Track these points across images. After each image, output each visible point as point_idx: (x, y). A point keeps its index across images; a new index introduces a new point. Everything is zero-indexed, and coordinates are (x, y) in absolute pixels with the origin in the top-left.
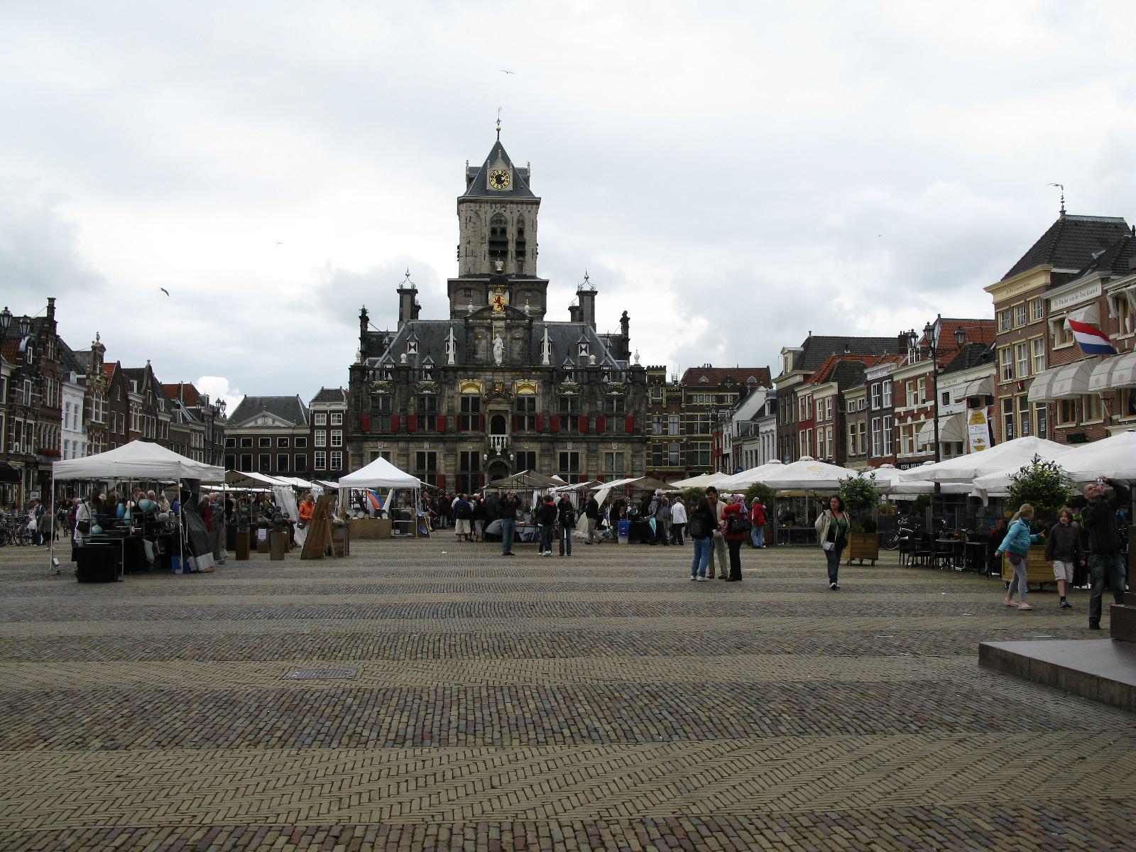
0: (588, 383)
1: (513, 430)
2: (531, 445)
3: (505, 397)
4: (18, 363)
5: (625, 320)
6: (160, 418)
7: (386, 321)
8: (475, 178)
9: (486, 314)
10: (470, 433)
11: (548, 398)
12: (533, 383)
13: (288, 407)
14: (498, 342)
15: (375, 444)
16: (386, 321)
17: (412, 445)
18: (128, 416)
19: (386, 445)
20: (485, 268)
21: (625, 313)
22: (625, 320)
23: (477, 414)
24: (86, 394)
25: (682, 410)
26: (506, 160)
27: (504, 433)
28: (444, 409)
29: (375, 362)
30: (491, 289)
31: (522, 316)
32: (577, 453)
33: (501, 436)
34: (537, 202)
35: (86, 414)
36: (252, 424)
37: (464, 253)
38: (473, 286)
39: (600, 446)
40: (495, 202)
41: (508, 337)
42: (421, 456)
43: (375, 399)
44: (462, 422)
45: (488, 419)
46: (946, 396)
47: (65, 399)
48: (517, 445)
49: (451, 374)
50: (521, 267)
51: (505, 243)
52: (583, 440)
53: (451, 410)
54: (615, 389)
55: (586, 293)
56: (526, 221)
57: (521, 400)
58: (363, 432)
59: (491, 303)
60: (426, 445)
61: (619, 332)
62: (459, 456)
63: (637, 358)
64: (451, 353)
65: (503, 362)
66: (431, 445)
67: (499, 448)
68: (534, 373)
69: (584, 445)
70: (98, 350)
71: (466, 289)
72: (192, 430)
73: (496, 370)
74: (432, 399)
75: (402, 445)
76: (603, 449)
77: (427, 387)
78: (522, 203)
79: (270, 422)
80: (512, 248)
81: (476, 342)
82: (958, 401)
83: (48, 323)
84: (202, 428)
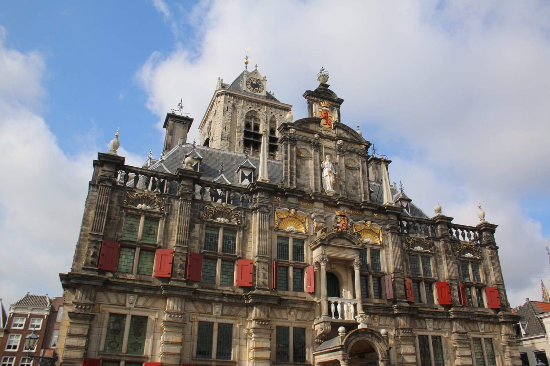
3: (350, 240)
9: (312, 127)
12: (377, 228)
14: (327, 164)
15: (121, 297)
17: (191, 307)
23: (299, 264)
28: (253, 249)
30: (317, 102)
42: (205, 329)
58: (102, 271)
66: (226, 311)
68: (376, 215)
73: (330, 203)
74: (230, 229)
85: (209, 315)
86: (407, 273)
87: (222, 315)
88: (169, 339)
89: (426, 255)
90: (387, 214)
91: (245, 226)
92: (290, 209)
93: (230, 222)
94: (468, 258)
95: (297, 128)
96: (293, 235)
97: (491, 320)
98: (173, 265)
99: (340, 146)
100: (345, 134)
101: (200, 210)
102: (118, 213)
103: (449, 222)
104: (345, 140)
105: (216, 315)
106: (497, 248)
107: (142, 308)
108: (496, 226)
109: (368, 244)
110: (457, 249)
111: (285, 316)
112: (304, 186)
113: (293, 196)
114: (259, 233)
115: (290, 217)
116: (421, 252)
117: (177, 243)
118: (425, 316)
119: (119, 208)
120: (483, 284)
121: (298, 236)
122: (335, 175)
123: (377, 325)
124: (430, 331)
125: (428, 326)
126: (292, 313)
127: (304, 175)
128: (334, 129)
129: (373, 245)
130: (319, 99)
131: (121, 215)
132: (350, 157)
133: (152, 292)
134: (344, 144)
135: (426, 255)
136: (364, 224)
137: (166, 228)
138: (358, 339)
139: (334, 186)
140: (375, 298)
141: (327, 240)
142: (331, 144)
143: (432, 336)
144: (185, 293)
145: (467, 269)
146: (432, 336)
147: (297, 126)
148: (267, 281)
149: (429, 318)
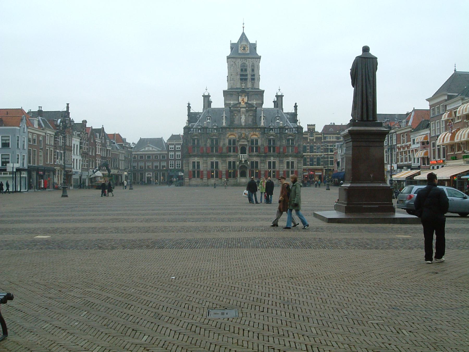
1: (249, 152)
3: (246, 139)
4: (57, 129)
5: (296, 107)
6: (107, 148)
7: (198, 107)
8: (234, 47)
9: (238, 105)
10: (232, 153)
11: (263, 139)
12: (257, 133)
13: (158, 142)
16: (198, 107)
17: (209, 159)
18: (96, 148)
20: (239, 86)
21: (296, 104)
22: (296, 107)
24: (81, 140)
25: (322, 143)
26: (247, 40)
28: (221, 144)
29: (194, 125)
31: (252, 106)
34: (259, 58)
35: (81, 148)
36: (143, 149)
37: (230, 79)
38: (234, 93)
39: (284, 158)
40: (242, 58)
41: (247, 115)
42: (212, 163)
43: (194, 140)
44: (229, 149)
45: (239, 149)
46: (414, 140)
47: (73, 142)
48: (251, 158)
49: (224, 130)
50: (253, 85)
51: (247, 75)
52: (278, 156)
53: (224, 145)
54: (290, 135)
55: (279, 96)
56: (255, 66)
57: (252, 141)
59: (240, 101)
60: (214, 159)
61: (294, 111)
63: (299, 123)
64: (224, 121)
65: (245, 125)
67: (243, 160)
69: (278, 158)
70: (85, 122)
71: (231, 94)
72: (120, 153)
73: (242, 128)
75: (205, 158)
76: (285, 160)
77: (214, 135)
78: (253, 58)
79: (151, 149)
80: (249, 77)
82: (418, 143)
83: (67, 113)
84: (124, 152)
105: (214, 159)
139: (245, 121)
142: (244, 109)
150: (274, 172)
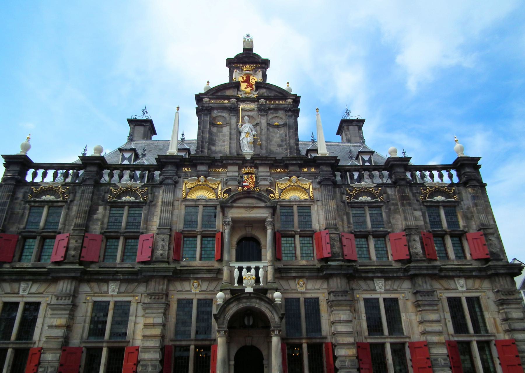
0: (394, 184)
2: (311, 285)
9: (229, 93)
11: (333, 204)
12: (307, 184)
14: (246, 127)
15: (15, 285)
17: (85, 288)
19: (35, 288)
27: (259, 259)
30: (237, 68)
32: (396, 300)
33: (253, 264)
42: (100, 308)
62: (174, 307)
66: (123, 289)
68: (305, 170)
81: (214, 130)
85: (104, 295)
86: (349, 227)
87: (119, 292)
88: (53, 322)
89: (374, 204)
90: (317, 166)
91: (151, 202)
92: (199, 177)
93: (136, 199)
94: (438, 202)
95: (210, 97)
96: (203, 203)
97: (474, 274)
98: (67, 249)
99: (262, 105)
100: (268, 92)
101: (105, 193)
102: (21, 208)
103: (405, 163)
104: (267, 98)
106: (485, 185)
107: (36, 294)
108: (479, 159)
109: (295, 201)
110: (421, 193)
111: (188, 288)
112: (220, 152)
113: (202, 164)
114: (162, 206)
115: (200, 185)
116: (368, 202)
117: (75, 227)
118: (370, 275)
119: (23, 203)
120: (463, 231)
121: (208, 203)
122: (254, 136)
123: (303, 289)
124: (380, 293)
125: (377, 288)
126: (195, 284)
127: (221, 141)
128: (257, 89)
129: (300, 201)
130: (241, 65)
131: (24, 209)
132: (274, 115)
133: (43, 277)
134: (266, 102)
135: (374, 204)
136: (289, 180)
137: (67, 214)
138: (241, 306)
140: (302, 260)
141: (230, 201)
143: (385, 299)
144: (73, 275)
145: (439, 216)
146: (385, 299)
147: (212, 95)
148: (167, 253)
149: (378, 277)
150: (398, 350)
